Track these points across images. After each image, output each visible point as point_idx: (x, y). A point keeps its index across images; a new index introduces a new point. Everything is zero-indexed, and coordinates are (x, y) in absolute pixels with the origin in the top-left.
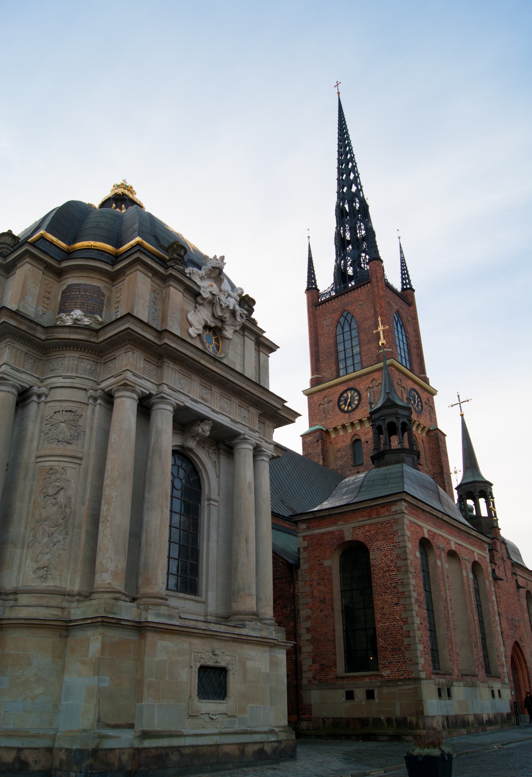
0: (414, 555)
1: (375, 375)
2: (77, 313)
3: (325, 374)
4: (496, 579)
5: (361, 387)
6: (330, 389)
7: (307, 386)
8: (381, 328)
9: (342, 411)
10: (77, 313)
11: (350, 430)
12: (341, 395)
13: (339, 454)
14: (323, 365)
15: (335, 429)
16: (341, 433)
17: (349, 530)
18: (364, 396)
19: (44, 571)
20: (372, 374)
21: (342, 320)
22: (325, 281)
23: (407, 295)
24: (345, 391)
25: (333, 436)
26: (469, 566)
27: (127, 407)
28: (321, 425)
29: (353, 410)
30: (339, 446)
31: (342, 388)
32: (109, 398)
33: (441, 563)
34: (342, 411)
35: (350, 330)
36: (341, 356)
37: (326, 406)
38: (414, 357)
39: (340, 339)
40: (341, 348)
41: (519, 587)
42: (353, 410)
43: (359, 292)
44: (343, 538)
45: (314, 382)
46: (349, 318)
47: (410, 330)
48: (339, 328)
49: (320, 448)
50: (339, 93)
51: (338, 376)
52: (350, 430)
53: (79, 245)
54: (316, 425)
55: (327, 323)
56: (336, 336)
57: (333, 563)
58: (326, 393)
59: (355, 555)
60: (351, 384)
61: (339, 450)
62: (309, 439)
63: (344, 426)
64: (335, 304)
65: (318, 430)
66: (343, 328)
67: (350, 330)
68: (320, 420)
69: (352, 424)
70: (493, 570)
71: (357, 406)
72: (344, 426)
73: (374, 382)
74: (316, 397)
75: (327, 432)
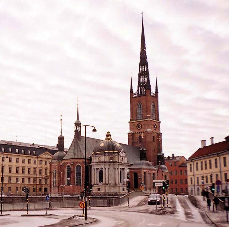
0: (143, 174)
1: (145, 122)
2: (111, 160)
4: (157, 175)
5: (142, 124)
7: (130, 121)
8: (143, 135)
9: (138, 129)
10: (111, 160)
11: (139, 134)
12: (137, 125)
13: (136, 139)
14: (133, 115)
15: (136, 133)
16: (137, 134)
17: (135, 171)
18: (143, 126)
19: (112, 182)
21: (139, 104)
22: (135, 90)
24: (139, 124)
25: (135, 134)
26: (152, 174)
27: (117, 169)
29: (140, 129)
30: (136, 137)
31: (138, 123)
32: (115, 168)
33: (147, 175)
34: (138, 129)
35: (141, 107)
36: (138, 114)
38: (156, 113)
39: (138, 109)
40: (138, 111)
41: (163, 175)
42: (140, 129)
44: (134, 172)
45: (131, 120)
46: (140, 104)
47: (156, 105)
48: (138, 106)
51: (137, 120)
52: (139, 134)
53: (110, 152)
55: (135, 103)
57: (133, 175)
58: (134, 123)
59: (136, 175)
60: (140, 123)
61: (136, 138)
62: (129, 134)
63: (138, 133)
64: (137, 99)
65: (131, 133)
66: (139, 106)
67: (141, 107)
68: (132, 130)
69: (140, 132)
70: (157, 174)
71: (141, 128)
72: (138, 133)
75: (134, 133)
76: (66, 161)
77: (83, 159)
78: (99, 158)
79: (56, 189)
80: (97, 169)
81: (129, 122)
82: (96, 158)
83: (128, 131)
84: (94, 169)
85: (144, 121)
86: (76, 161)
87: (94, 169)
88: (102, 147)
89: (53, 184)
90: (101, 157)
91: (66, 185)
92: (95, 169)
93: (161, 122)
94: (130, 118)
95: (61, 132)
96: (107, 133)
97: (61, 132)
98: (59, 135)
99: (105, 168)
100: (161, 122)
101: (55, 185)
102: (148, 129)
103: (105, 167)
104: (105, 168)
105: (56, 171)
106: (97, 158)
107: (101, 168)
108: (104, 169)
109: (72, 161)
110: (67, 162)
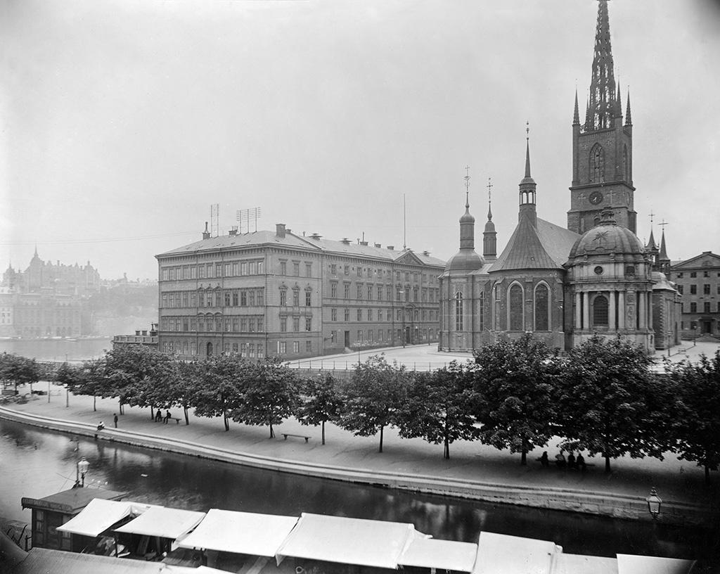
23: (628, 130)
32: (638, 293)
62: (572, 215)
80: (590, 293)
81: (570, 189)
84: (582, 294)
87: (582, 294)
91: (508, 329)
92: (586, 296)
93: (634, 189)
95: (467, 207)
97: (467, 207)
98: (463, 213)
99: (617, 293)
100: (634, 189)
101: (461, 328)
105: (463, 297)
107: (608, 292)
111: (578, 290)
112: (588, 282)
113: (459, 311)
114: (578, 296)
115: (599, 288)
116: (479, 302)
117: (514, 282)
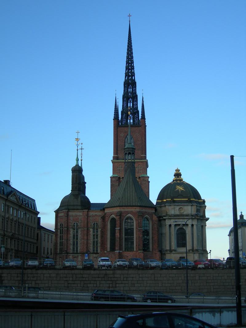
1: (140, 163)
3: (120, 156)
6: (122, 163)
20: (138, 163)
25: (121, 180)
28: (118, 175)
37: (120, 168)
43: (136, 128)
49: (118, 183)
50: (130, 21)
54: (115, 174)
56: (125, 142)
65: (116, 177)
73: (139, 166)
74: (116, 164)
75: (119, 178)
76: (124, 210)
77: (153, 209)
78: (180, 208)
79: (79, 257)
80: (176, 225)
82: (174, 208)
83: (111, 174)
84: (170, 226)
85: (139, 162)
86: (144, 210)
88: (182, 191)
89: (72, 248)
90: (185, 208)
91: (124, 250)
92: (173, 226)
94: (112, 155)
96: (176, 170)
99: (192, 225)
102: (144, 174)
103: (194, 223)
104: (192, 225)
106: (177, 208)
108: (190, 226)
109: (138, 209)
110: (127, 212)
111: (168, 222)
112: (176, 216)
113: (75, 237)
114: (168, 226)
115: (181, 222)
116: (91, 230)
117: (128, 215)
